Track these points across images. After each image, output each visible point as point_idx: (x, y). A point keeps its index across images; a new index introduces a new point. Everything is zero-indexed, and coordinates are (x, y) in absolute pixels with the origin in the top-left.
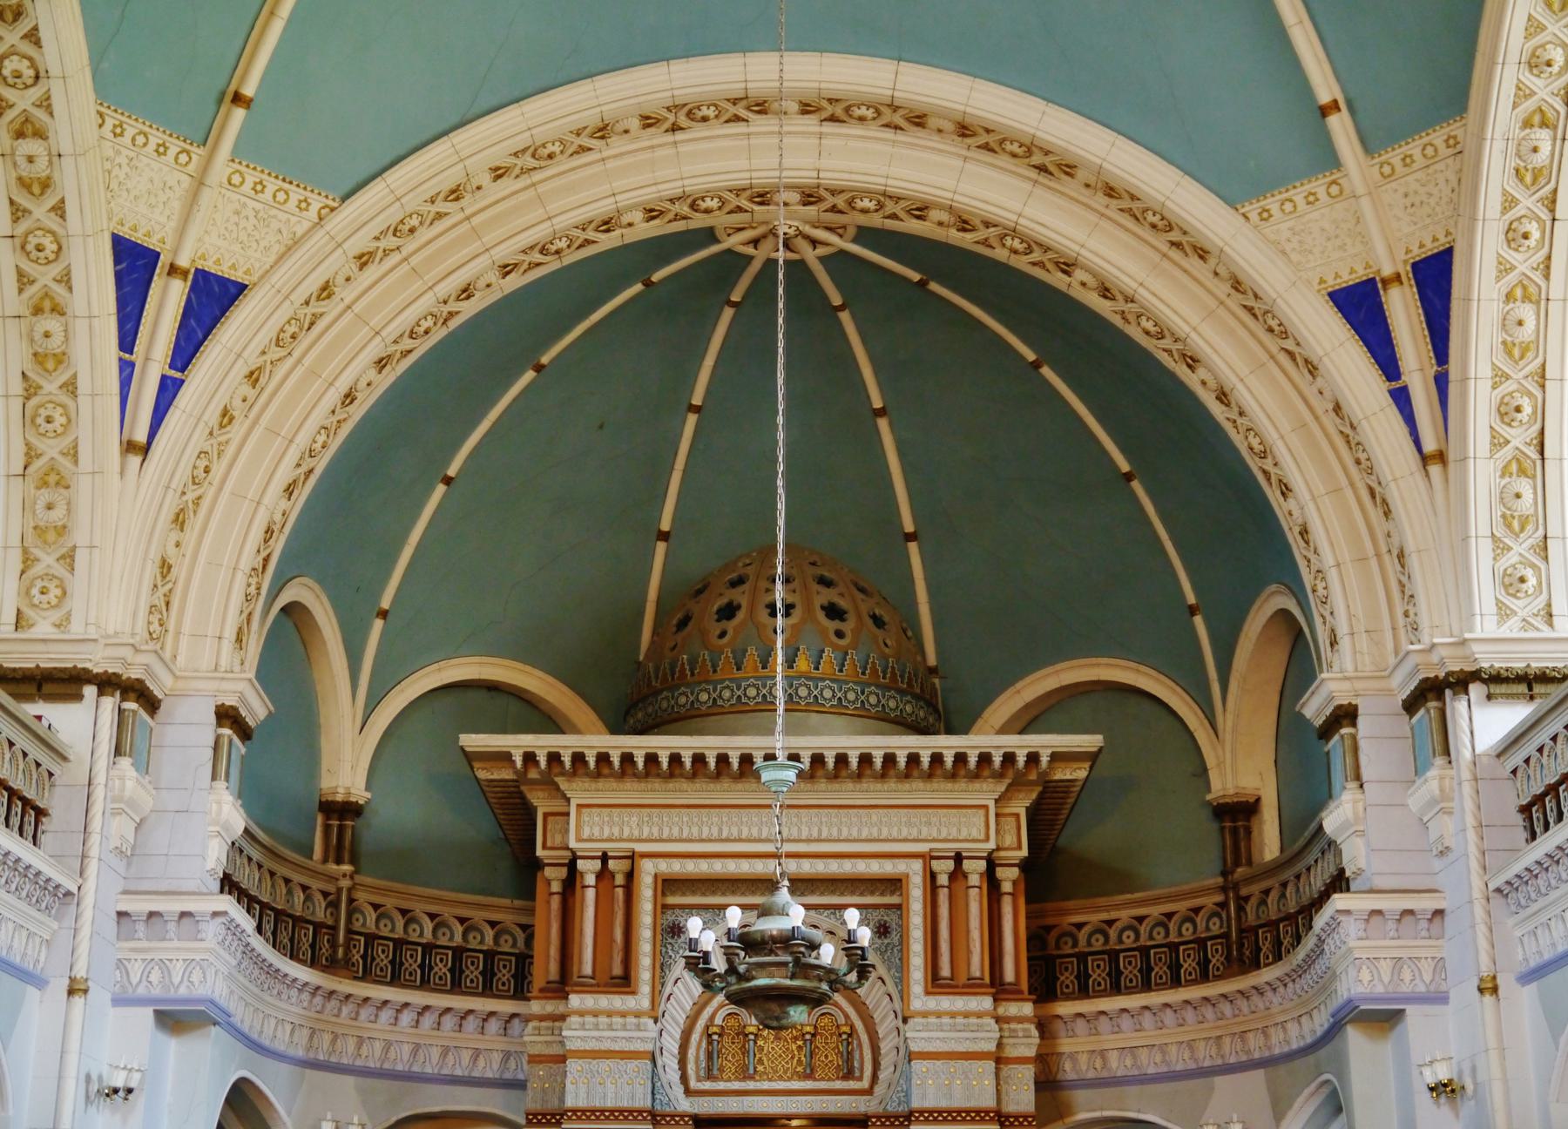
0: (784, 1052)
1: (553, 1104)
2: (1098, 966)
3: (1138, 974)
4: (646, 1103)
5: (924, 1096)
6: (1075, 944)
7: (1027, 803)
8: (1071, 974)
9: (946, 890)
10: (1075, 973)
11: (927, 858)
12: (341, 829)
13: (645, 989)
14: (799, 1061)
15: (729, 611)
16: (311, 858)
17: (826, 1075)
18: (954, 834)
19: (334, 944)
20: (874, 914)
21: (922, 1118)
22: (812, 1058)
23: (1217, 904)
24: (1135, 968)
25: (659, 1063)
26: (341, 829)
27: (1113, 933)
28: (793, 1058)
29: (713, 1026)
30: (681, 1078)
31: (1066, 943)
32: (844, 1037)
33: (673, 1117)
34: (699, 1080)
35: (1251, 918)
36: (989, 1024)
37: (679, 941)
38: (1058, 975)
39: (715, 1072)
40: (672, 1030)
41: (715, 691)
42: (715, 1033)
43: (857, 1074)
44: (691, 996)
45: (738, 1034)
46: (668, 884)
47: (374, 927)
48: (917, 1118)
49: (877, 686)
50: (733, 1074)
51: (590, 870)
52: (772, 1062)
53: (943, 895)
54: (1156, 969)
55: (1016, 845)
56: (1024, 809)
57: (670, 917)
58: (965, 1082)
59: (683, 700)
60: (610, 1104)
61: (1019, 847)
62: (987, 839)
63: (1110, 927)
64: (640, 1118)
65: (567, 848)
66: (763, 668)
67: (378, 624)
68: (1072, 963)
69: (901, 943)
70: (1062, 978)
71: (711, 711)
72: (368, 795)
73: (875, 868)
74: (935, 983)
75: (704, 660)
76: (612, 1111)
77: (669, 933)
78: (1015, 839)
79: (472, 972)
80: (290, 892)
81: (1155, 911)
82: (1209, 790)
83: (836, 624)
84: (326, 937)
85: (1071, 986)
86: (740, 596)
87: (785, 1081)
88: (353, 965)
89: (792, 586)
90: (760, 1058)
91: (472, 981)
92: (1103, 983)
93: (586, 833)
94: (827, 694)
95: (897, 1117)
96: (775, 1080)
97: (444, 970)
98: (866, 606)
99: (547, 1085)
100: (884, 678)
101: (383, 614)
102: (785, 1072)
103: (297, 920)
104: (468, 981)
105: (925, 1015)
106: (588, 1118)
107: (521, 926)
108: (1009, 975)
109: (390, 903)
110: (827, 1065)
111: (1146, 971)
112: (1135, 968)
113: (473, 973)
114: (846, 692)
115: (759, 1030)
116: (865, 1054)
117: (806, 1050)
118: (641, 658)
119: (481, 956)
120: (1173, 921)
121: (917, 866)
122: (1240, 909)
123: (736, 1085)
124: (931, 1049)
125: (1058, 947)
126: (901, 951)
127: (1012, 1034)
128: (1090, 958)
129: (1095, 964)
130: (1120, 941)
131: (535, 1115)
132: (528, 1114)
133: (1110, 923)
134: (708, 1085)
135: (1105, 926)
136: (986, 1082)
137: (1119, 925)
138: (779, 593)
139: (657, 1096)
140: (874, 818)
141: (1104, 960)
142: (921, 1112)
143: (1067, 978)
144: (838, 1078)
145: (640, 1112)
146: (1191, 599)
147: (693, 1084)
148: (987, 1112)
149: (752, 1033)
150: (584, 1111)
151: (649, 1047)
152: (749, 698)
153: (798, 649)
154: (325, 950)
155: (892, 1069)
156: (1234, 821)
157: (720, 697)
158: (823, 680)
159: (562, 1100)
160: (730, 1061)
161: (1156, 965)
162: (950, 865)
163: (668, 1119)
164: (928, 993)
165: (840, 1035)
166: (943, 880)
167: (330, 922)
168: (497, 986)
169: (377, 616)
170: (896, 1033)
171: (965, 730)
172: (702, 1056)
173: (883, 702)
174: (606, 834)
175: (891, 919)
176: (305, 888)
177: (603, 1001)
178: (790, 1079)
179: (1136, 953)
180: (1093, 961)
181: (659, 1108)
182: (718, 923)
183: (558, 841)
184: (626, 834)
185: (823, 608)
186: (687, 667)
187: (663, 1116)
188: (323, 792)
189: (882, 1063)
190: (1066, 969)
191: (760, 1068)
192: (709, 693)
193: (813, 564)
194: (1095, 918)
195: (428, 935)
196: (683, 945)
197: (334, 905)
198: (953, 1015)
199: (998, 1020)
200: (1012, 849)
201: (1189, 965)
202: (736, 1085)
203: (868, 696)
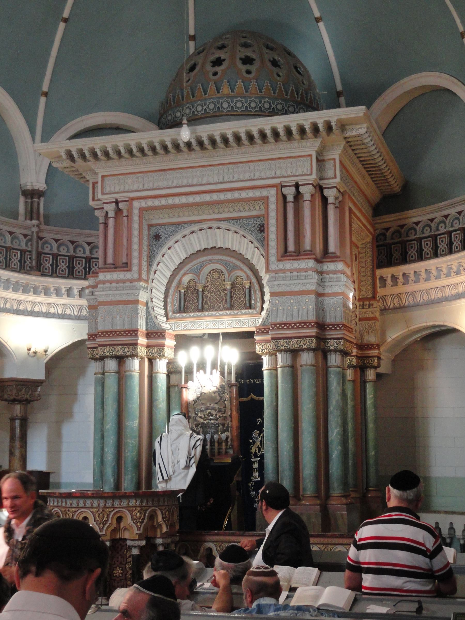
0: (218, 297)
7: (339, 152)
8: (414, 250)
10: (416, 249)
12: (32, 203)
13: (135, 268)
14: (226, 301)
20: (258, 220)
21: (276, 328)
24: (444, 244)
26: (32, 203)
28: (222, 300)
31: (412, 233)
33: (157, 333)
37: (159, 242)
38: (408, 251)
48: (331, 329)
49: (269, 98)
51: (110, 208)
54: (455, 243)
55: (333, 176)
56: (315, 152)
57: (154, 231)
60: (119, 328)
61: (335, 177)
64: (134, 334)
70: (410, 252)
73: (251, 194)
77: (154, 239)
83: (248, 67)
84: (29, 256)
90: (206, 301)
92: (429, 253)
94: (239, 105)
98: (268, 55)
106: (109, 335)
108: (332, 248)
109: (64, 238)
110: (240, 303)
112: (444, 244)
114: (250, 103)
121: (273, 192)
125: (407, 236)
127: (330, 280)
129: (426, 243)
131: (91, 336)
133: (432, 220)
136: (311, 307)
137: (436, 221)
141: (430, 241)
143: (412, 252)
148: (310, 323)
150: (107, 332)
158: (236, 97)
162: (293, 189)
166: (290, 198)
167: (29, 249)
168: (76, 274)
169: (42, 95)
173: (273, 106)
174: (117, 190)
176: (11, 233)
177: (115, 276)
180: (425, 241)
182: (178, 232)
184: (127, 189)
185: (241, 59)
186: (172, 100)
191: (206, 306)
194: (425, 218)
200: (333, 178)
203: (263, 104)
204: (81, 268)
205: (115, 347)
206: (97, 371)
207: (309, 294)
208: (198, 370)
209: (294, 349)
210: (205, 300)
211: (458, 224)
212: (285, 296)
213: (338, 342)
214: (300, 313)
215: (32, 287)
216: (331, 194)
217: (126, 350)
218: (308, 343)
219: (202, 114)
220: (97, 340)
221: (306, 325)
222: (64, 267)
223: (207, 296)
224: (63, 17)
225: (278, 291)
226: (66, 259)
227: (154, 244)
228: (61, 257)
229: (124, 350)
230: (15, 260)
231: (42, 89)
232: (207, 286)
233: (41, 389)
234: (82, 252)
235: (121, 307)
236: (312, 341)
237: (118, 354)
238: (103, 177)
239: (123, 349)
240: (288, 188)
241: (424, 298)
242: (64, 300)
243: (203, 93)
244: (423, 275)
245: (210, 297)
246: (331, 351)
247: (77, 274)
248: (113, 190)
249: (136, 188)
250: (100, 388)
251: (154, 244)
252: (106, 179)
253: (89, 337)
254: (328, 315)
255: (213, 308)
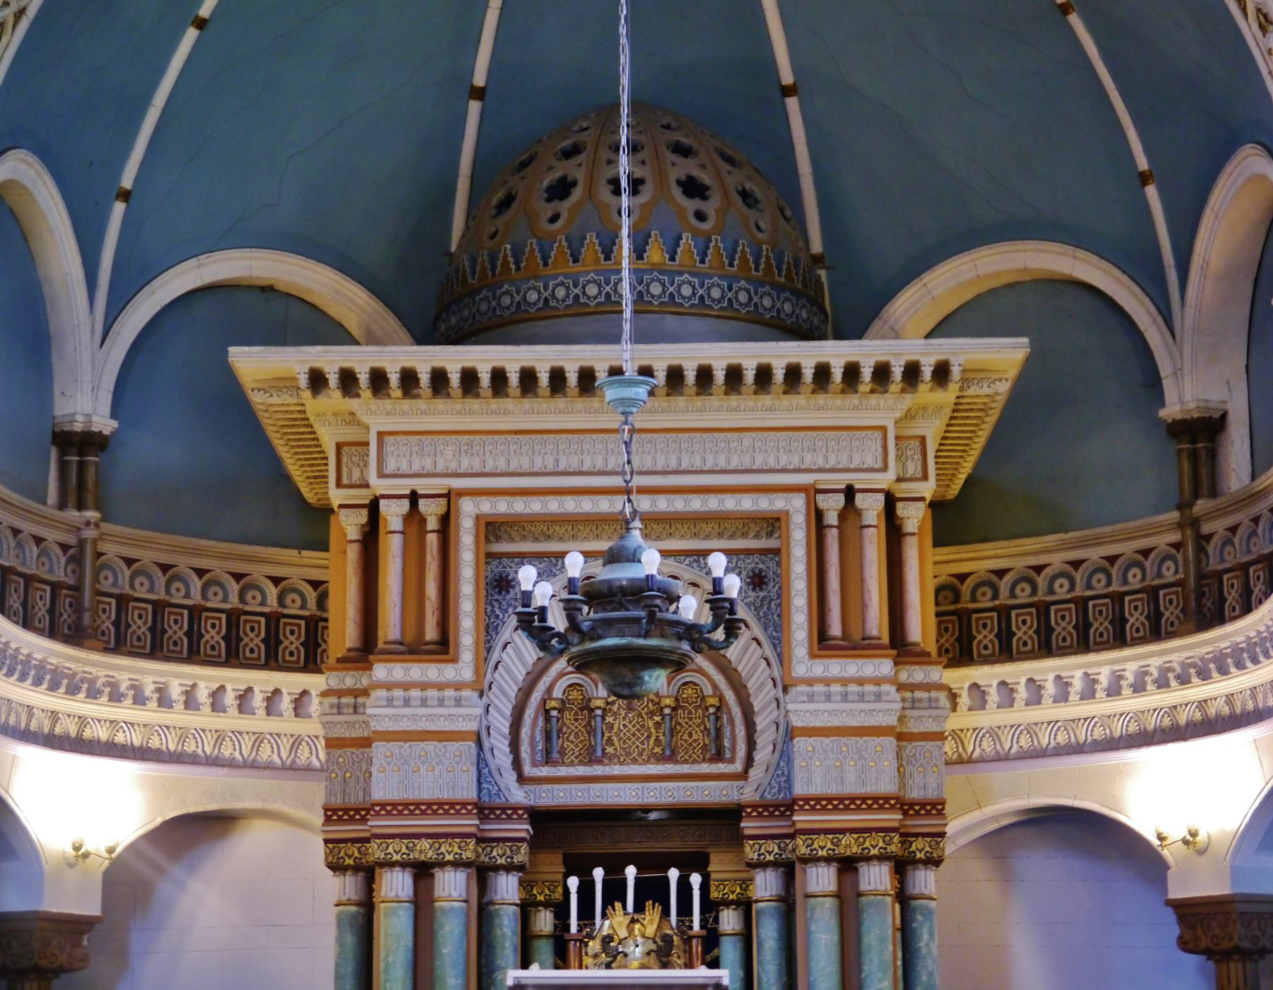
0: (638, 730)
1: (355, 798)
2: (1024, 622)
3: (1074, 632)
4: (470, 793)
5: (809, 782)
6: (995, 596)
8: (991, 632)
9: (835, 532)
10: (996, 631)
11: (812, 492)
13: (467, 656)
14: (657, 739)
15: (561, 189)
16: (45, 503)
17: (690, 756)
18: (844, 462)
19: (78, 609)
21: (807, 807)
22: (672, 736)
23: (1171, 545)
25: (486, 745)
26: (82, 466)
27: (1041, 581)
28: (649, 737)
29: (551, 699)
30: (513, 764)
31: (984, 594)
32: (712, 710)
33: (504, 810)
34: (534, 764)
35: (1214, 564)
36: (888, 694)
37: (508, 597)
38: (974, 633)
39: (555, 755)
40: (500, 705)
41: (546, 289)
42: (554, 708)
43: (728, 755)
44: (524, 664)
45: (582, 709)
46: (492, 528)
47: (127, 587)
49: (748, 280)
50: (576, 757)
52: (625, 742)
53: (832, 537)
54: (1096, 625)
57: (495, 566)
58: (859, 763)
59: (506, 301)
60: (425, 795)
61: (925, 477)
62: (885, 468)
63: (1039, 574)
64: (464, 811)
65: (367, 486)
66: (605, 260)
67: (119, 208)
68: (991, 618)
69: (779, 597)
70: (979, 637)
71: (542, 314)
72: (115, 424)
73: (747, 504)
74: (822, 642)
75: (532, 250)
76: (429, 805)
77: (495, 588)
78: (919, 468)
79: (252, 640)
80: (20, 546)
81: (1094, 554)
82: (1162, 403)
84: (68, 600)
85: (990, 646)
86: (575, 169)
87: (640, 764)
88: (103, 633)
89: (641, 156)
90: (609, 737)
91: (252, 651)
92: (1030, 643)
93: (391, 466)
94: (686, 291)
95: (777, 807)
96: (628, 764)
97: (217, 638)
98: (734, 179)
99: (348, 775)
100: (756, 270)
101: (125, 196)
102: (640, 754)
103: (28, 579)
104: (247, 651)
105: (810, 682)
106: (400, 813)
107: (310, 582)
109: (147, 556)
110: (690, 744)
111: (1083, 627)
112: (1069, 623)
113: (253, 640)
114: (709, 289)
115: (608, 703)
116: (737, 731)
117: (666, 726)
118: (453, 248)
119: (263, 620)
120: (1116, 566)
121: (797, 504)
122: (1201, 550)
123: (581, 771)
124: (818, 724)
125: (974, 599)
126: (779, 605)
128: (1013, 613)
129: (1020, 619)
130: (1051, 591)
131: (335, 811)
132: (326, 810)
133: (1039, 569)
134: (545, 771)
135: (1033, 574)
137: (1049, 571)
138: (624, 163)
139: (485, 785)
140: (746, 442)
141: (1030, 614)
142: (807, 800)
144: (704, 760)
145: (464, 805)
146: (1143, 164)
147: (528, 770)
148: (887, 799)
149: (599, 708)
150: (395, 805)
151: (473, 726)
152: (589, 298)
153: (650, 236)
154: (66, 616)
155: (771, 747)
156: (1194, 441)
157: (553, 296)
158: (681, 273)
159: (367, 791)
160: (572, 742)
161: (1096, 619)
162: (840, 500)
163: (498, 812)
164: (813, 656)
165: (706, 708)
166: (832, 518)
167: (71, 581)
170: (775, 704)
171: (858, 333)
172: (538, 737)
173: (756, 299)
174: (416, 468)
175: (767, 566)
177: (417, 671)
178: (647, 762)
179: (1072, 606)
181: (487, 800)
182: (555, 575)
183: (356, 474)
184: (440, 467)
185: (679, 183)
187: (492, 809)
188: (58, 420)
189: (758, 741)
190: (985, 626)
191: (610, 750)
192: (539, 292)
193: (667, 127)
195: (196, 598)
196: (513, 603)
197: (77, 560)
198: (845, 682)
199: (901, 687)
201: (1136, 619)
202: (581, 771)
203: (737, 293)
204: (180, 634)
205: (416, 841)
206: (344, 898)
207: (882, 735)
208: (608, 902)
209: (848, 857)
210: (607, 735)
211: (1104, 582)
212: (827, 736)
213: (933, 843)
214: (863, 776)
215: (82, 680)
216: (914, 517)
217: (443, 850)
218: (881, 844)
219: (600, 304)
220: (370, 823)
221: (878, 804)
222: (142, 630)
223: (611, 727)
224: (197, 16)
225: (811, 725)
226: (299, 626)
227: (497, 600)
228: (136, 604)
229: (439, 848)
230: (41, 609)
231: (119, 183)
232: (613, 703)
233: (88, 940)
234: (183, 592)
235: (430, 746)
236: (892, 839)
237: (423, 858)
238: (381, 435)
239: (437, 845)
240: (830, 495)
241: (1022, 743)
242: (150, 714)
243: (602, 256)
244: (1022, 693)
245: (619, 729)
246: (805, 861)
247: (172, 648)
248: (405, 468)
249: (465, 466)
250: (350, 940)
251: (497, 600)
252: (387, 439)
253: (329, 813)
254: (911, 782)
255: (628, 754)
